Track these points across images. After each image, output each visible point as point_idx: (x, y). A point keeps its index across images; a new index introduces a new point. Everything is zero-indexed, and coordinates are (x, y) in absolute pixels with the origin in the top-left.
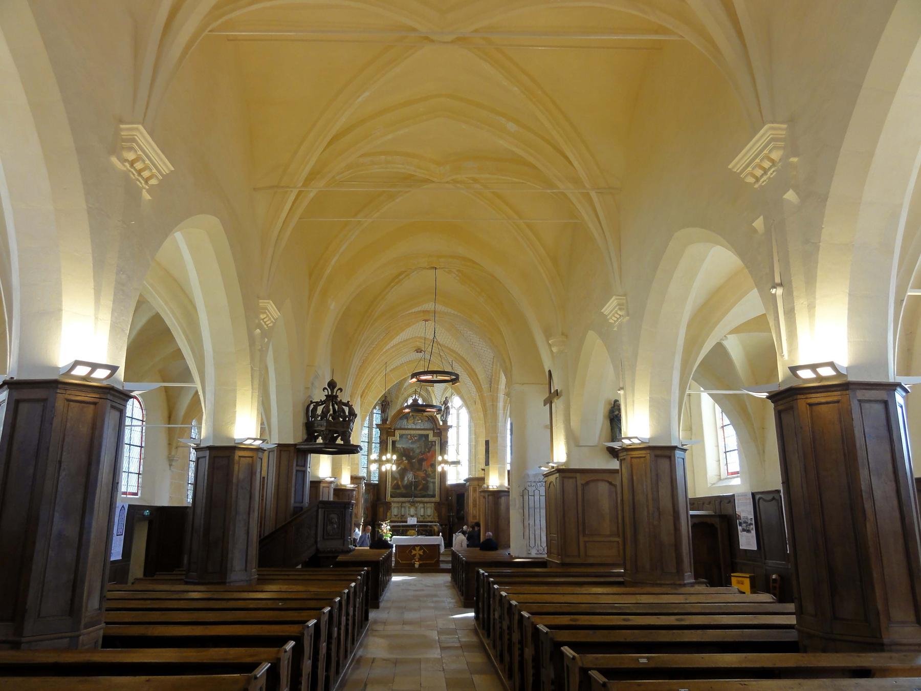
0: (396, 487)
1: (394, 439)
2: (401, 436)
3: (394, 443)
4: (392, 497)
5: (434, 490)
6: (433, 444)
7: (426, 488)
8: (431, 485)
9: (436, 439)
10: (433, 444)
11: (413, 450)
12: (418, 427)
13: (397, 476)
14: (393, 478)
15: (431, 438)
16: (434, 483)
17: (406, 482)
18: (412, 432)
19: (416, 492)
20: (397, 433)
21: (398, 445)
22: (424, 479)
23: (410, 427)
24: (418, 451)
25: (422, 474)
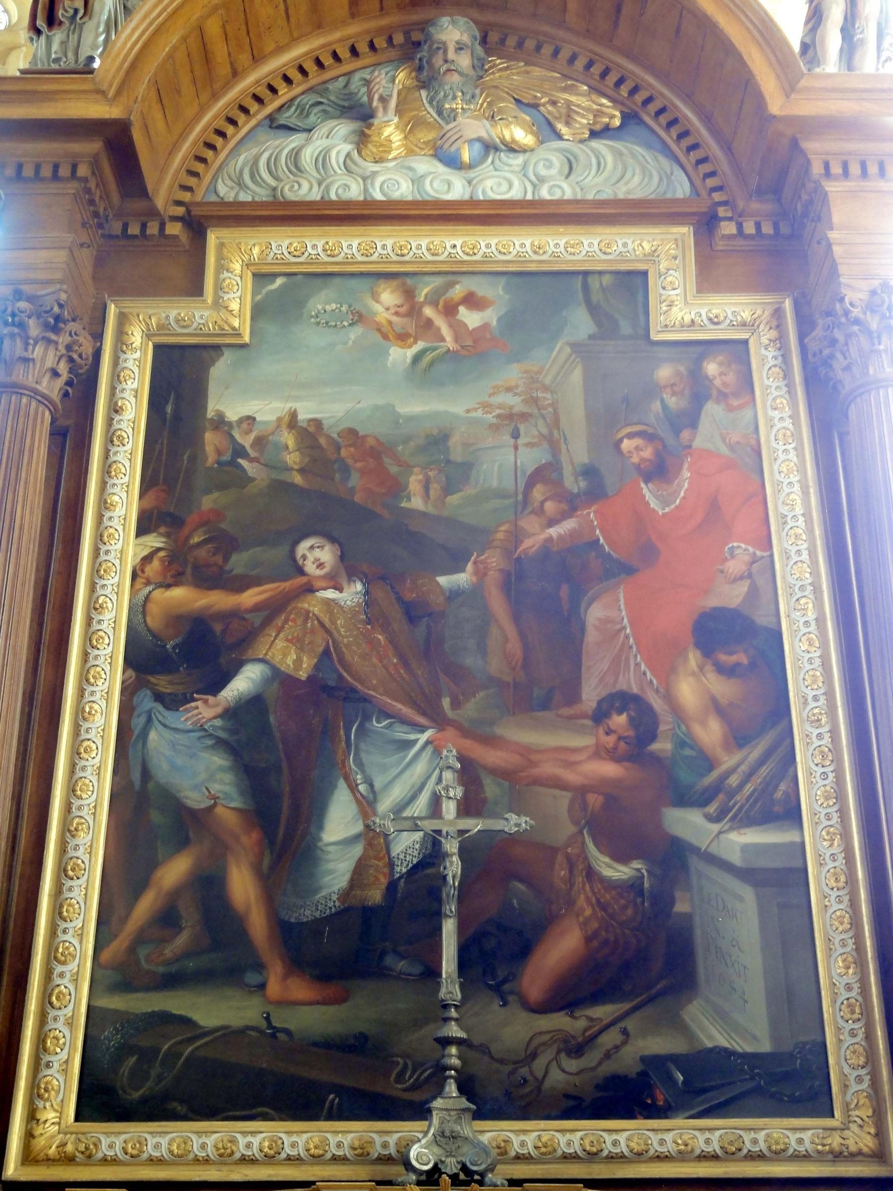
0: (175, 938)
1: (188, 318)
2: (284, 296)
3: (179, 375)
4: (99, 1100)
5: (796, 995)
6: (713, 368)
7: (648, 958)
8: (733, 928)
9: (735, 310)
10: (713, 368)
11: (437, 442)
12: (499, 183)
13: (203, 777)
14: (145, 815)
15: (682, 307)
16: (784, 882)
17: (336, 870)
18: (422, 245)
19: (513, 1028)
20: (235, 263)
21: (245, 401)
22: (618, 822)
23: (393, 183)
24: (503, 464)
25: (574, 753)
